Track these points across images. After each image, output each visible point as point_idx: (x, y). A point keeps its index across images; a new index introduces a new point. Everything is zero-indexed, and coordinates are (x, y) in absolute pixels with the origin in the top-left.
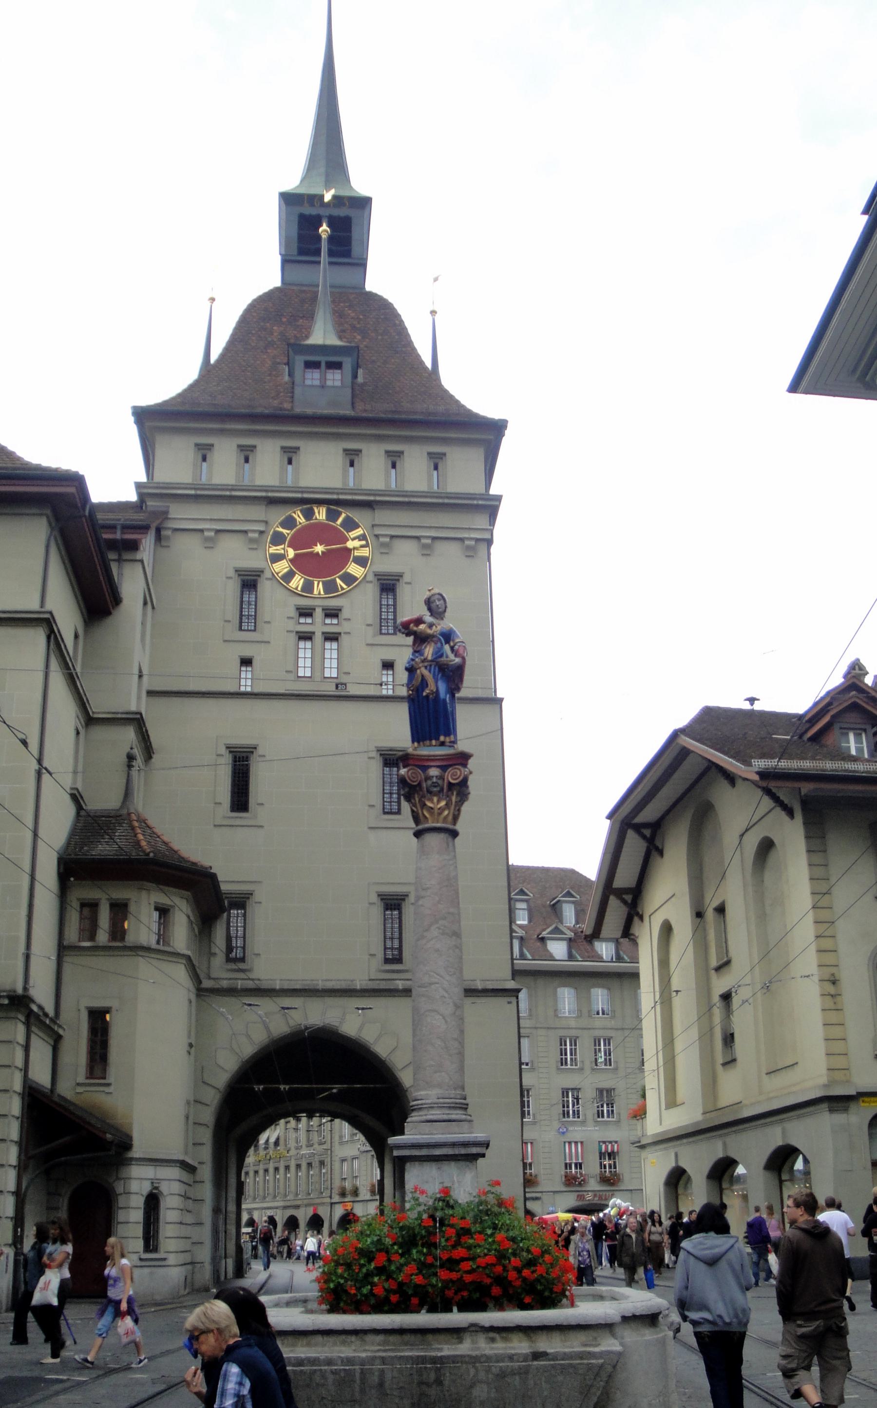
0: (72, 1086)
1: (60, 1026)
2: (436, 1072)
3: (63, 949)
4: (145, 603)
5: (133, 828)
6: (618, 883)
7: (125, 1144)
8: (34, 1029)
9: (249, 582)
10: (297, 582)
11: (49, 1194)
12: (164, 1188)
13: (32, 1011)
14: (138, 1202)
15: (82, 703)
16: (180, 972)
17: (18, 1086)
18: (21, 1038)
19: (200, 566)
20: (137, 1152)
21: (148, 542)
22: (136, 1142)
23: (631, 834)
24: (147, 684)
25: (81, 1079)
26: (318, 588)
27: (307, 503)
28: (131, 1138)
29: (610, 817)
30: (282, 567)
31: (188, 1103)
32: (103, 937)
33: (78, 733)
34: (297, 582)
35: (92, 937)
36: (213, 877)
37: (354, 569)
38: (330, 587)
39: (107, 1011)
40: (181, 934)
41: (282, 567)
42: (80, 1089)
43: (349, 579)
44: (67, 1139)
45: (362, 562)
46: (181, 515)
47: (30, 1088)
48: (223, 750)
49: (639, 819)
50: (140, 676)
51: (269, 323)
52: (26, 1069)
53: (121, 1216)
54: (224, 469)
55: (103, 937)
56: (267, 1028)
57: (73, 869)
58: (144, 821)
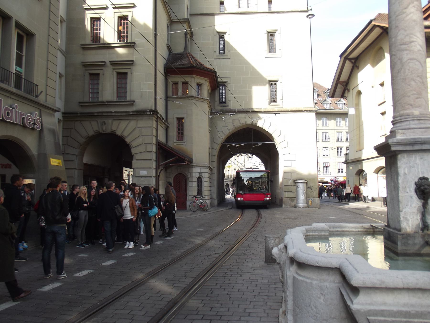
0: (173, 143)
1: (168, 123)
2: (417, 98)
3: (167, 98)
5: (188, 58)
6: (342, 79)
7: (191, 161)
8: (159, 123)
11: (167, 177)
12: (203, 175)
14: (195, 179)
15: (169, 16)
17: (154, 141)
18: (155, 126)
20: (194, 164)
22: (194, 160)
23: (348, 62)
28: (192, 159)
29: (341, 56)
31: (209, 148)
32: (180, 94)
33: (168, 27)
35: (177, 93)
39: (183, 118)
42: (175, 144)
44: (172, 159)
49: (351, 56)
53: (190, 184)
55: (180, 94)
56: (233, 125)
57: (169, 71)
58: (192, 55)
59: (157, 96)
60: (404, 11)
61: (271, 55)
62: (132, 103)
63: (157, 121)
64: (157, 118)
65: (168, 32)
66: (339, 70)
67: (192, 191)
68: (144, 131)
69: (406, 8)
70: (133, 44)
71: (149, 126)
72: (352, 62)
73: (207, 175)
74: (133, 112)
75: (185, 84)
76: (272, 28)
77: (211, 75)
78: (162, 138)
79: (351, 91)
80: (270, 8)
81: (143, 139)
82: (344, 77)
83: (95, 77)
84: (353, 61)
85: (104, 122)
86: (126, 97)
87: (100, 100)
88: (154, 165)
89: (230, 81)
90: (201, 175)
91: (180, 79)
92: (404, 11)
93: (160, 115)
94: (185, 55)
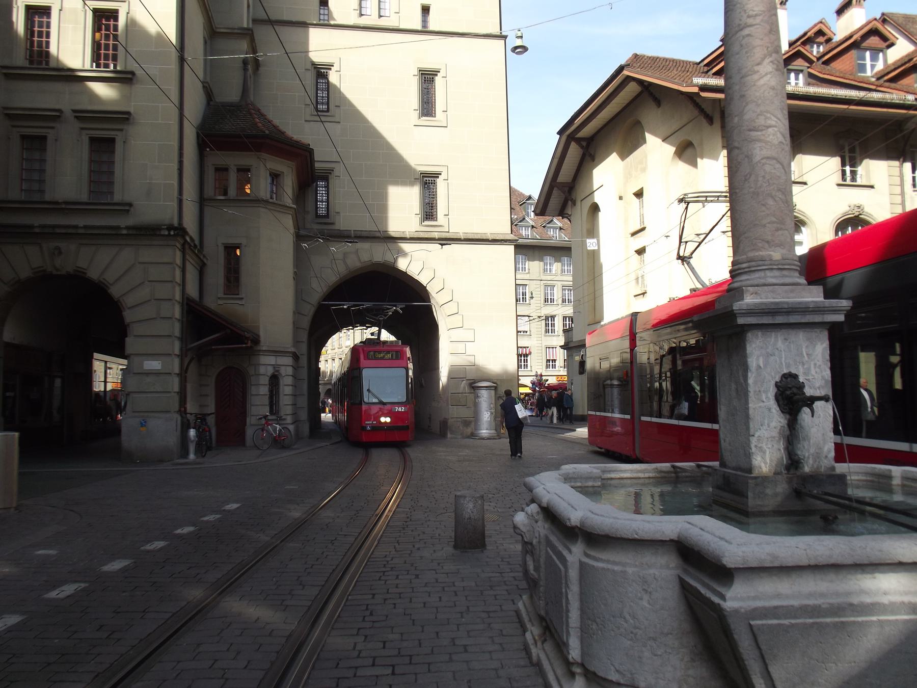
0: (216, 301)
1: (204, 256)
3: (203, 201)
5: (251, 114)
7: (256, 341)
8: (187, 257)
12: (283, 371)
13: (186, 241)
14: (265, 380)
16: (288, 221)
17: (178, 296)
18: (178, 261)
20: (264, 346)
22: (262, 339)
23: (573, 145)
25: (221, 295)
28: (259, 336)
33: (205, 42)
35: (225, 193)
36: (311, 152)
42: (220, 302)
47: (188, 299)
49: (581, 135)
53: (253, 390)
56: (345, 263)
59: (185, 197)
60: (756, 68)
61: (425, 120)
62: (126, 208)
64: (183, 245)
65: (205, 55)
66: (556, 161)
67: (258, 405)
69: (758, 64)
70: (130, 76)
71: (165, 260)
72: (582, 147)
73: (290, 371)
74: (128, 228)
75: (244, 171)
76: (429, 65)
77: (301, 155)
78: (192, 290)
79: (578, 203)
80: (425, 22)
81: (152, 290)
82: (565, 176)
83: (36, 143)
84: (584, 144)
85: (58, 249)
86: (112, 193)
87: (47, 198)
88: (177, 347)
89: (339, 170)
90: (278, 371)
91: (233, 160)
92: (756, 68)
93: (191, 238)
94: (244, 108)
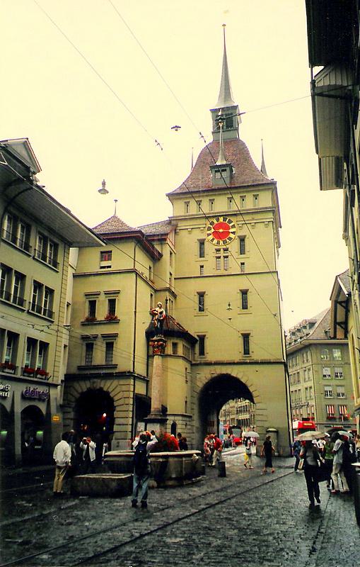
4: (171, 253)
9: (202, 243)
10: (215, 241)
17: (132, 396)
18: (132, 383)
19: (188, 240)
21: (171, 237)
24: (173, 276)
26: (221, 242)
27: (217, 217)
30: (211, 237)
34: (215, 241)
37: (232, 236)
38: (225, 242)
40: (180, 351)
41: (211, 237)
43: (230, 239)
45: (234, 233)
46: (182, 225)
48: (196, 294)
50: (171, 274)
51: (206, 160)
52: (134, 391)
54: (193, 209)
57: (149, 334)
62: (115, 366)
63: (134, 380)
68: (124, 388)
74: (116, 373)
83: (90, 347)
86: (112, 361)
87: (93, 364)
